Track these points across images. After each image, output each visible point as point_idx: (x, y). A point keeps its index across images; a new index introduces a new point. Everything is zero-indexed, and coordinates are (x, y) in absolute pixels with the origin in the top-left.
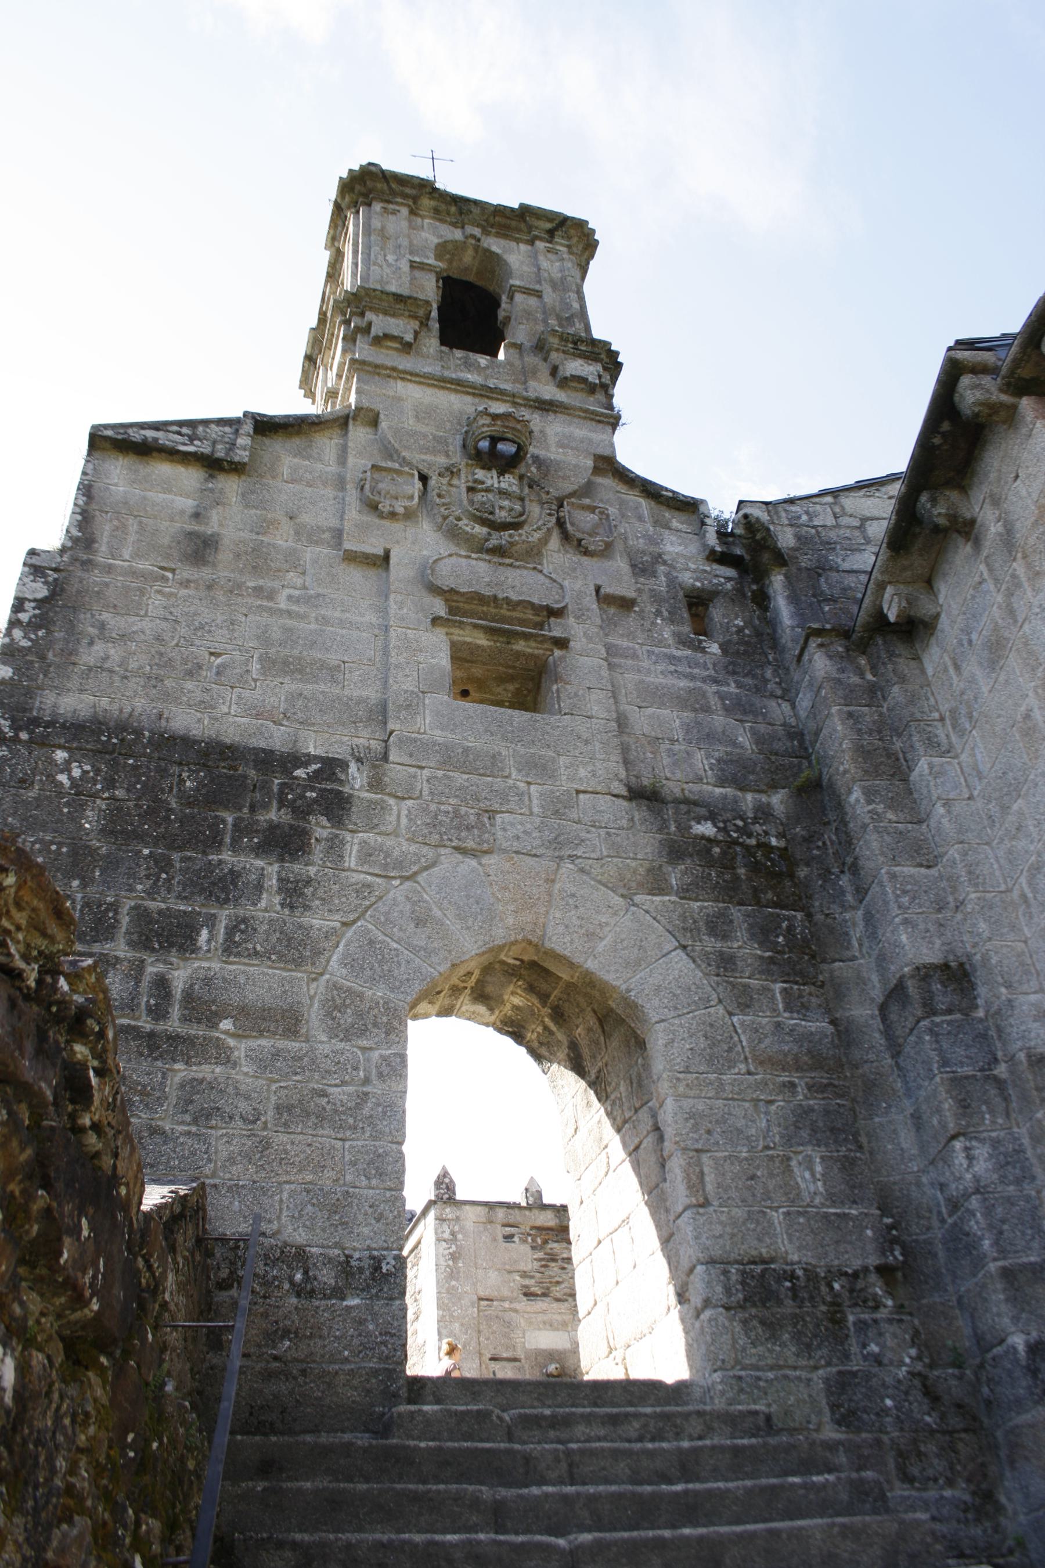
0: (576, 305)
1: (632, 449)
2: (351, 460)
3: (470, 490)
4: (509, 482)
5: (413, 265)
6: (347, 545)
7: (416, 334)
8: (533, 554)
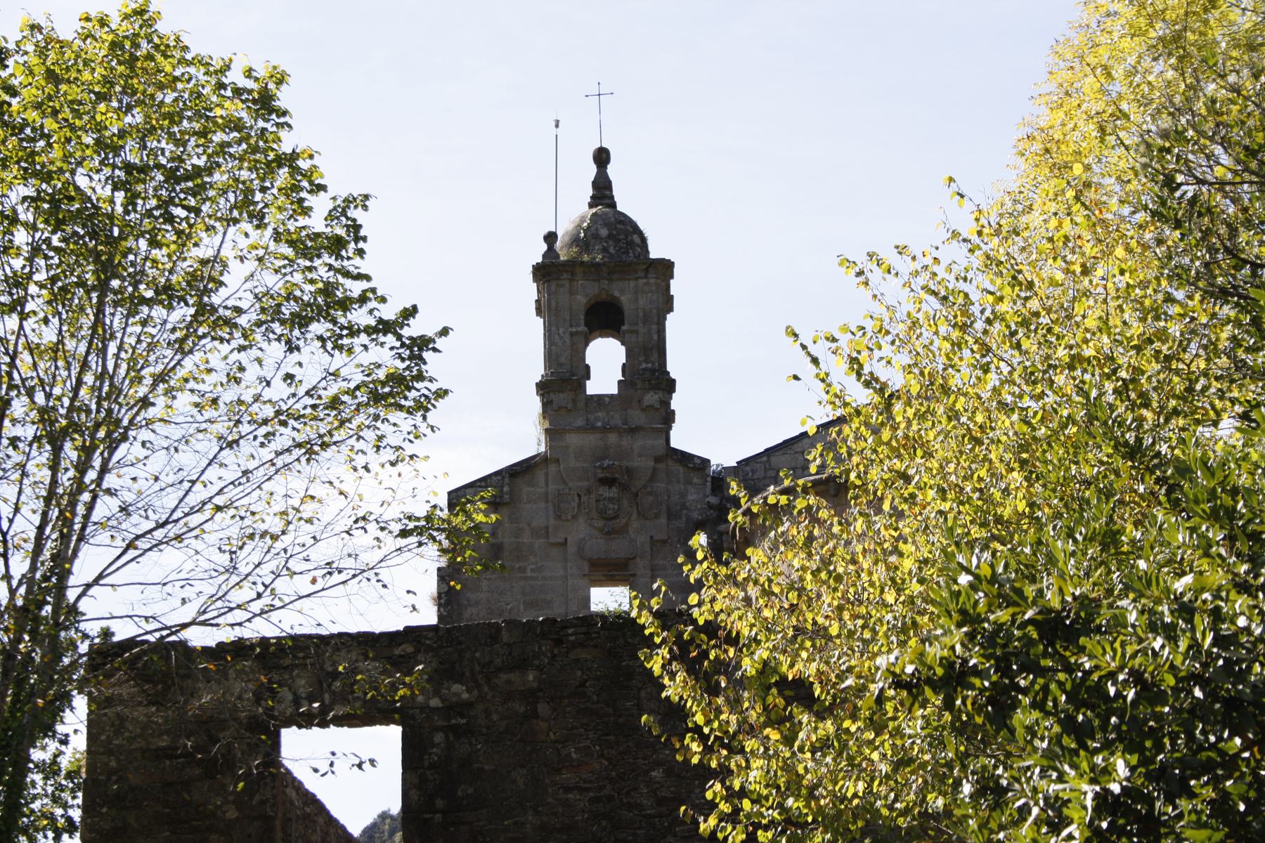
0: (655, 337)
1: (681, 438)
2: (551, 487)
3: (597, 501)
4: (613, 492)
5: (572, 334)
6: (551, 540)
7: (574, 401)
8: (623, 531)
